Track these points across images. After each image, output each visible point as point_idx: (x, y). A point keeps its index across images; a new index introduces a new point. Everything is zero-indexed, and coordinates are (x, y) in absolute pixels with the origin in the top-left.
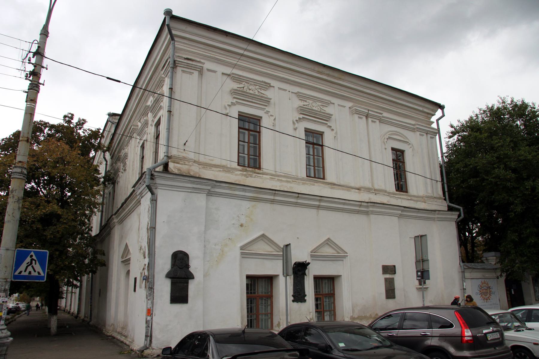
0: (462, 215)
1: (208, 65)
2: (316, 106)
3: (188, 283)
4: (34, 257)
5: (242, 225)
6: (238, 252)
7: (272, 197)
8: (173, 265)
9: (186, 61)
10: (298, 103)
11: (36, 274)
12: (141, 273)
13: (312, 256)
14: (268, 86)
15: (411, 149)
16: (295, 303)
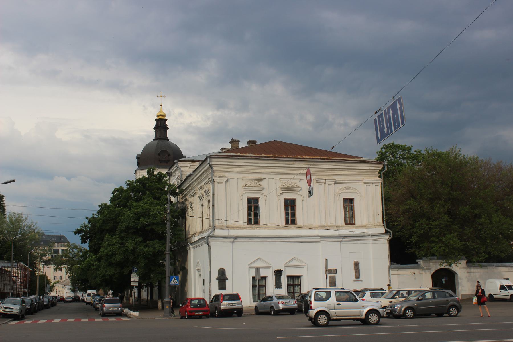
0: (392, 237)
2: (291, 184)
3: (225, 281)
4: (175, 278)
9: (219, 178)
10: (280, 184)
11: (176, 283)
13: (285, 266)
15: (359, 196)
16: (276, 289)
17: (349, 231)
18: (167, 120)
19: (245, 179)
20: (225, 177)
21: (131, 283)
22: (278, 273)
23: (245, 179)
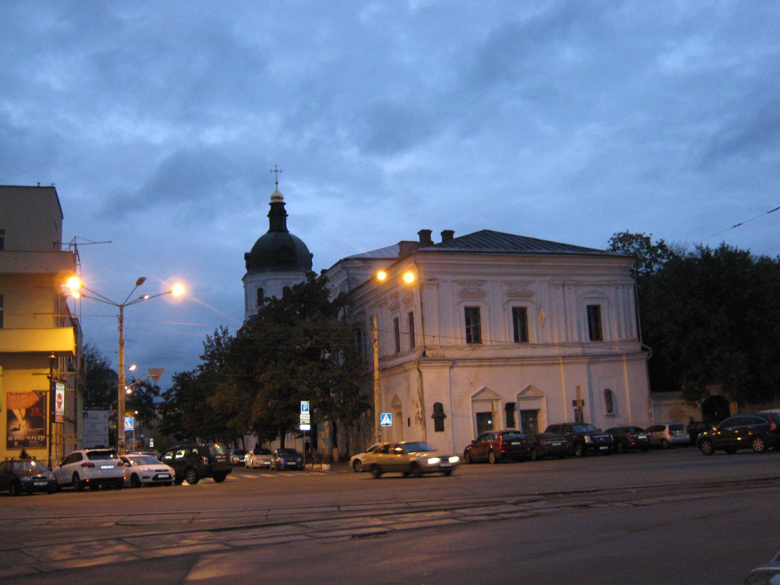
1: (441, 277)
5: (471, 383)
6: (470, 399)
7: (489, 364)
8: (435, 410)
10: (506, 288)
12: (416, 416)
14: (483, 282)
17: (597, 349)
18: (285, 204)
19: (461, 283)
20: (437, 279)
21: (301, 426)
22: (510, 408)
23: (461, 283)
